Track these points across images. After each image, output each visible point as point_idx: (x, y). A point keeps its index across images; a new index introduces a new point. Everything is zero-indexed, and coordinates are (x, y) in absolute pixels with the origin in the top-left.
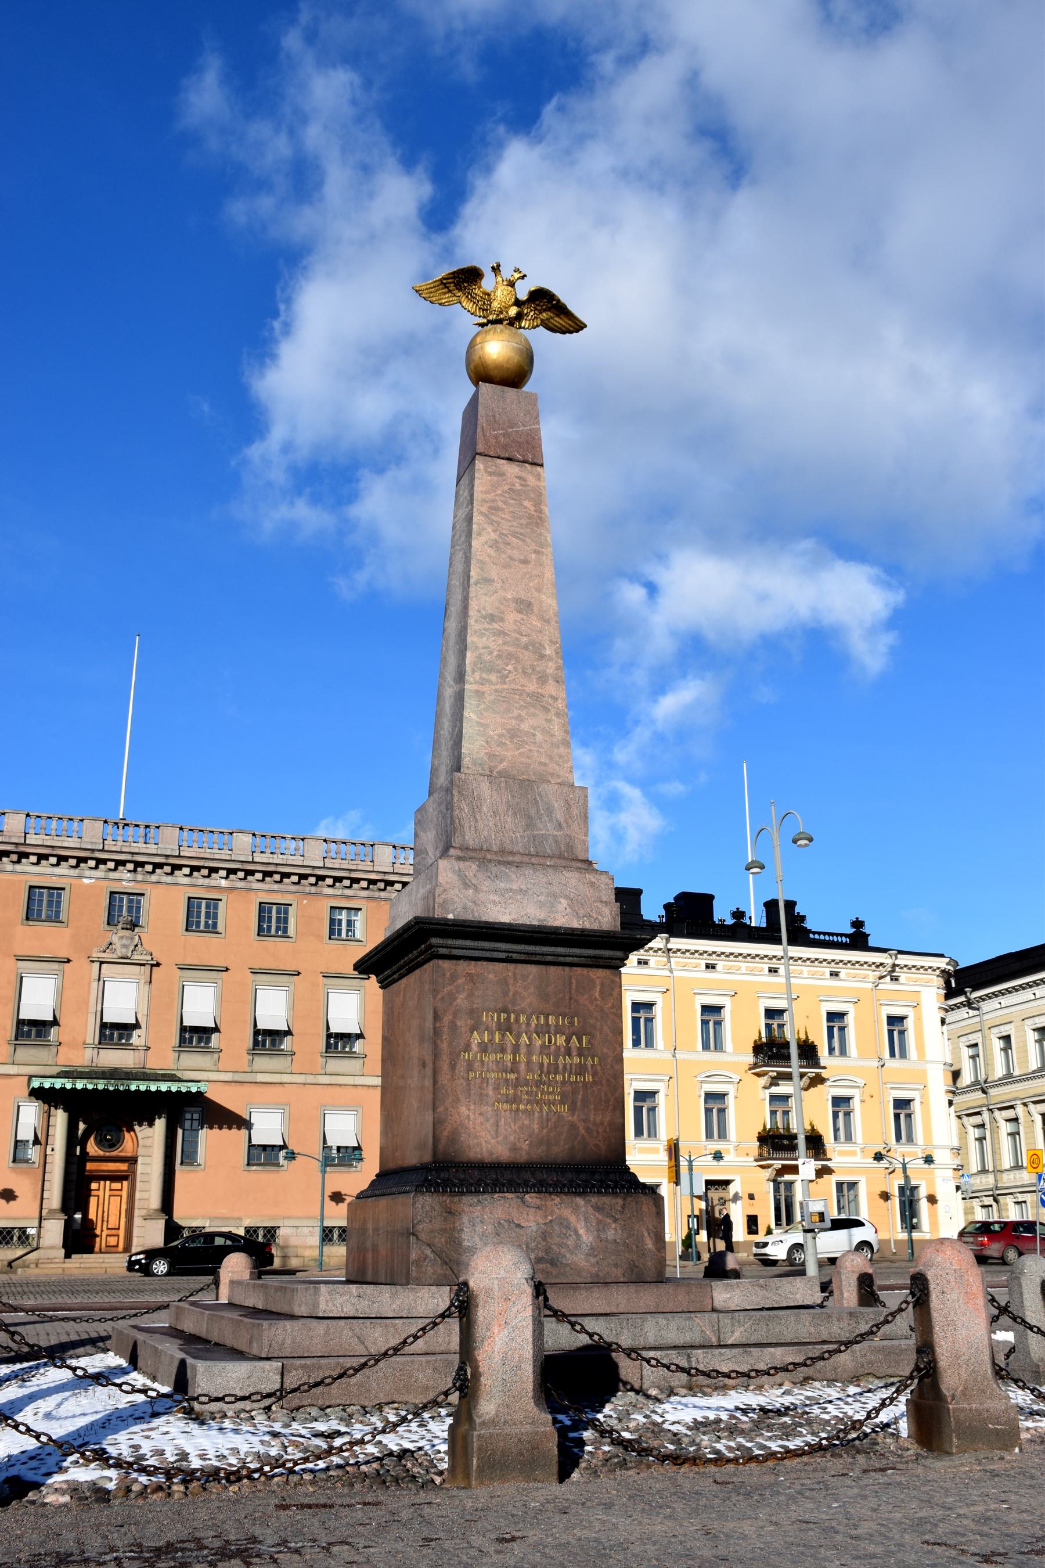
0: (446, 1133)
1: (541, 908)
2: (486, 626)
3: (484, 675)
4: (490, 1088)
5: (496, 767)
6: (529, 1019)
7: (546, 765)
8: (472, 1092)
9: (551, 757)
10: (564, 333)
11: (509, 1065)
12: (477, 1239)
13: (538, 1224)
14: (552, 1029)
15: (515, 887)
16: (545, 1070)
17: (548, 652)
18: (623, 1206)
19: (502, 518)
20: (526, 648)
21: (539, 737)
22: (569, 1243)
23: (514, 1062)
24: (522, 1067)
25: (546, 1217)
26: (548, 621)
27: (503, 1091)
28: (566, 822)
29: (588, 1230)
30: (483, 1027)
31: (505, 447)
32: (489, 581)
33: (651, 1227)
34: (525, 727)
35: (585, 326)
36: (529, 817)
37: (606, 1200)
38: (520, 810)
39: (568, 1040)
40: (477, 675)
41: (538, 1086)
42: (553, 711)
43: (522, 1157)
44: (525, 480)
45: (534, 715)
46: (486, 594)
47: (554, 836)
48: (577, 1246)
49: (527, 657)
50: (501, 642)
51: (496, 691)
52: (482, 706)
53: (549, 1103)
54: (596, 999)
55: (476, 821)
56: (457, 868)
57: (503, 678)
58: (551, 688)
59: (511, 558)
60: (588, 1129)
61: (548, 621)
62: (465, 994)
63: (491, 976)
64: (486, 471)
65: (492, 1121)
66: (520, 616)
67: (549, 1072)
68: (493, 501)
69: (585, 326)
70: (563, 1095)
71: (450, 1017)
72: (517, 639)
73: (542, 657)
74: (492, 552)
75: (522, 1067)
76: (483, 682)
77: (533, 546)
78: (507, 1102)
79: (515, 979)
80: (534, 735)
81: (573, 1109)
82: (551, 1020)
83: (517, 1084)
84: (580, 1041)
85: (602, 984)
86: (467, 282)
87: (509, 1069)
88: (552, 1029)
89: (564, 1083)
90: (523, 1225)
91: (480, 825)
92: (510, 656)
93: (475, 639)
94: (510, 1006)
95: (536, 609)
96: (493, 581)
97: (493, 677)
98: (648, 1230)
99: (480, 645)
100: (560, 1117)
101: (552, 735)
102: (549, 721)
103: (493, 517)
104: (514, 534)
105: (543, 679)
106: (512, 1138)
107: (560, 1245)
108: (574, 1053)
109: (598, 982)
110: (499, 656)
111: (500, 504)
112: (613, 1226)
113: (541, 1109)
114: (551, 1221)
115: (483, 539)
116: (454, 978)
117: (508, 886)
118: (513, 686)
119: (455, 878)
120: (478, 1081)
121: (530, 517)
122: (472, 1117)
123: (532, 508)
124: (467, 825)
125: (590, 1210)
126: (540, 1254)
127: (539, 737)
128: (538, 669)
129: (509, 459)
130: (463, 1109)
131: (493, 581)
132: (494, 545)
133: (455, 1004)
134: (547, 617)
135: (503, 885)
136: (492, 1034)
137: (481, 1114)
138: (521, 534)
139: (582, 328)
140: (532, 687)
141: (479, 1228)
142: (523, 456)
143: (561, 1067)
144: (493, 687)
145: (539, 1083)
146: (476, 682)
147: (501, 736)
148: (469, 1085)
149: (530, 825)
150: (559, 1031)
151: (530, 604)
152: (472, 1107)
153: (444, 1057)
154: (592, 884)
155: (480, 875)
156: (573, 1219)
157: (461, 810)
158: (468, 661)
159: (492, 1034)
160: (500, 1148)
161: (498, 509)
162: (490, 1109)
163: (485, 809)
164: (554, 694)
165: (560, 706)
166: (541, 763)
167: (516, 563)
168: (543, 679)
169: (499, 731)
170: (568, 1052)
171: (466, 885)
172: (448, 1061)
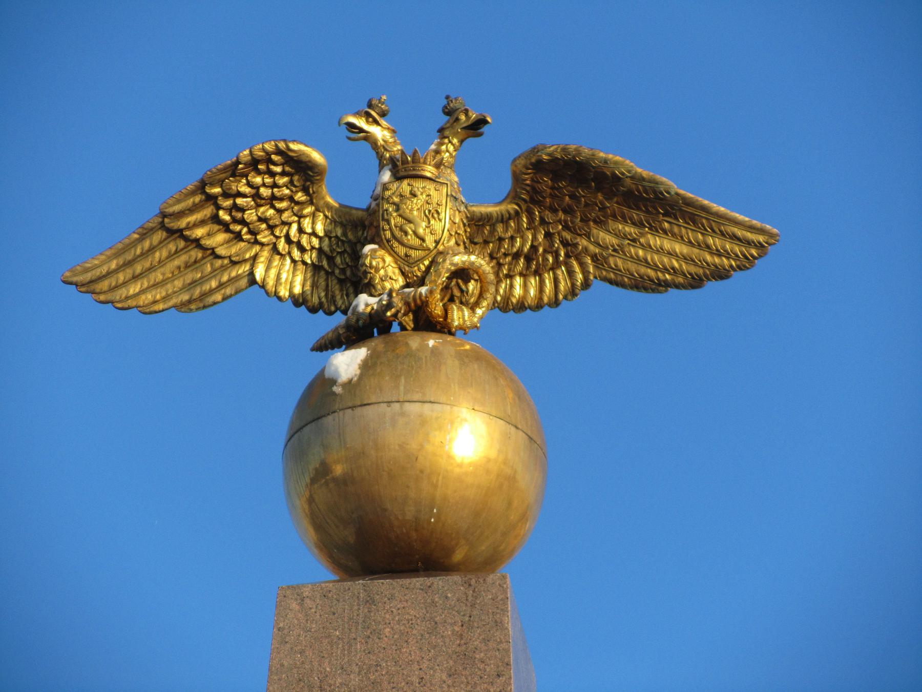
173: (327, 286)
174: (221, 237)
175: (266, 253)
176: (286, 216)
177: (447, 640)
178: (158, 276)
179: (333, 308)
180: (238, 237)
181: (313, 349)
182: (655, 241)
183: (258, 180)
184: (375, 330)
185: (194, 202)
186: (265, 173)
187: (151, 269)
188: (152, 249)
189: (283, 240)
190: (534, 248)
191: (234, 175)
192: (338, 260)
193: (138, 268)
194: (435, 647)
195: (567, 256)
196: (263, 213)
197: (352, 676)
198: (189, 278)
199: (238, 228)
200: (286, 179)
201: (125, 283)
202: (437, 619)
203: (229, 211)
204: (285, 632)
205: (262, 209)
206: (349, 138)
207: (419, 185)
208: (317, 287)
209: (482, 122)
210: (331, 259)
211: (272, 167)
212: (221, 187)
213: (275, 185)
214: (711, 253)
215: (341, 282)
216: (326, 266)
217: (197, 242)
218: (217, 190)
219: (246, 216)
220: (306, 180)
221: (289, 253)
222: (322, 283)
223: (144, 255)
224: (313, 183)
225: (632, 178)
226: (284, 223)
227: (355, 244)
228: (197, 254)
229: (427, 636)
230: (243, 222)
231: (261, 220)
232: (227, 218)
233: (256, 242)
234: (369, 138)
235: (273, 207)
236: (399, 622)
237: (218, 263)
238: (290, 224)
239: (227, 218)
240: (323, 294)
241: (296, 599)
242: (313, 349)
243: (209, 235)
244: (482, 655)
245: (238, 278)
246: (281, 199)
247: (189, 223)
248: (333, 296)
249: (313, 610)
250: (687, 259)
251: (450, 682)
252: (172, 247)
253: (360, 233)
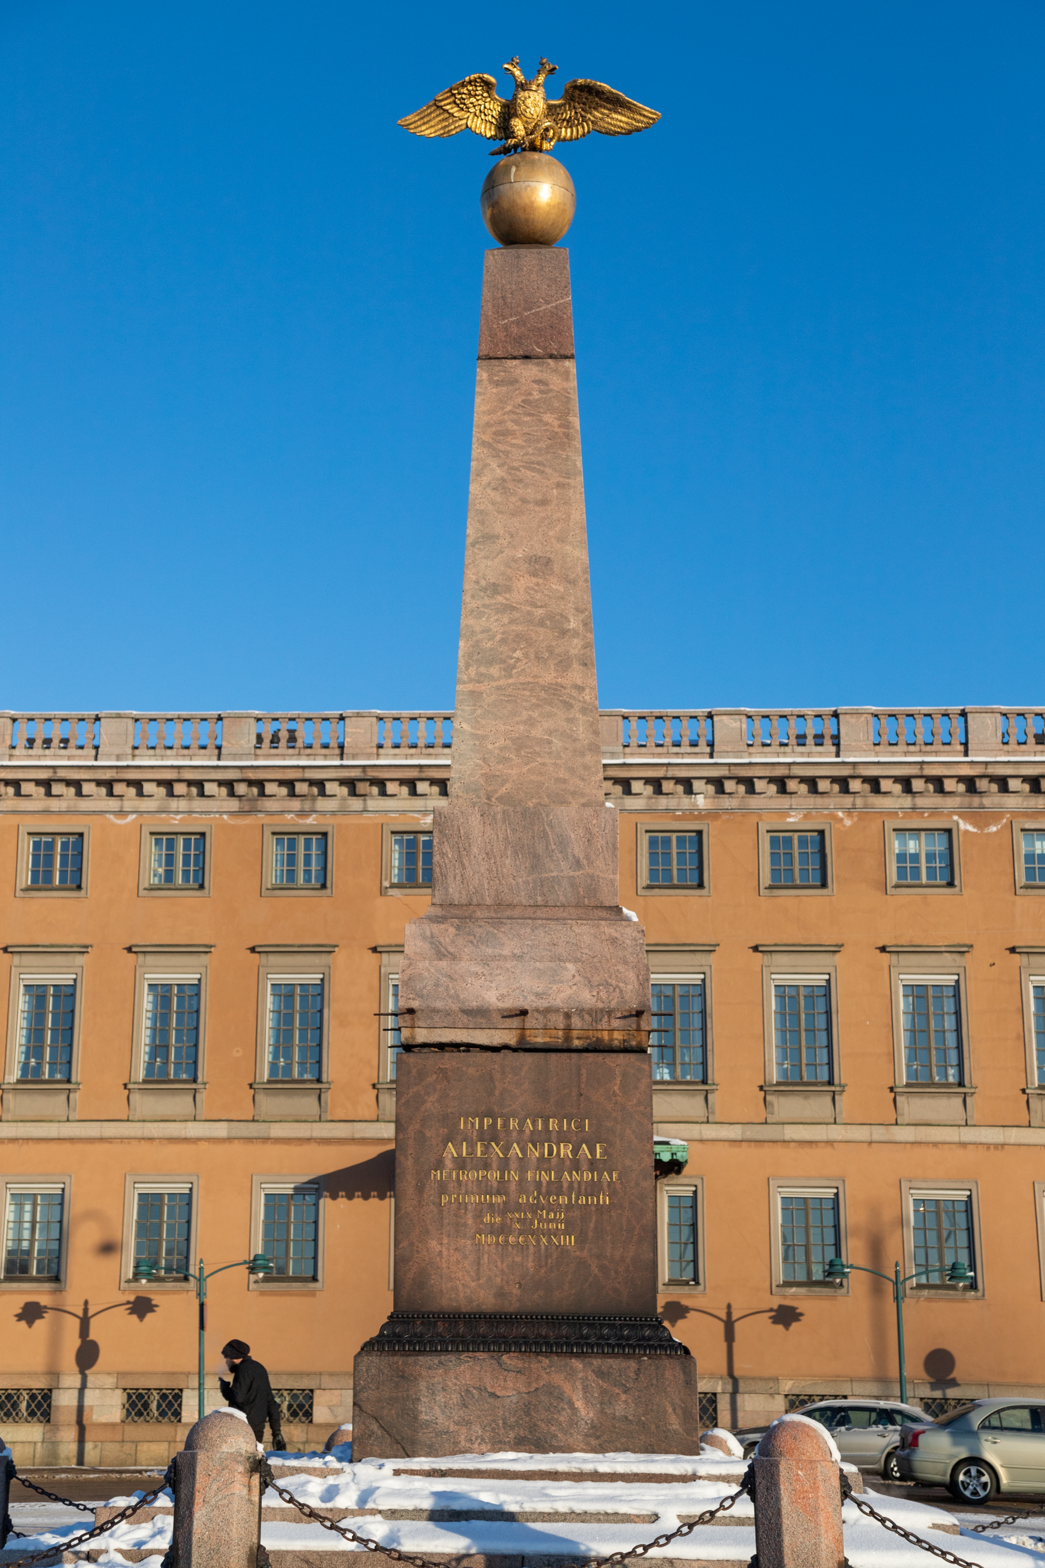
0: (410, 1275)
1: (539, 977)
2: (487, 601)
3: (483, 670)
4: (470, 1215)
5: (496, 791)
6: (522, 1124)
7: (564, 781)
8: (446, 1221)
9: (572, 770)
11: (495, 1185)
12: (437, 1411)
13: (519, 1393)
14: (554, 1136)
15: (506, 952)
16: (544, 1190)
17: (572, 625)
18: (638, 1372)
19: (513, 445)
20: (541, 623)
21: (557, 743)
22: (562, 1419)
23: (502, 1181)
24: (513, 1187)
25: (530, 1384)
26: (573, 582)
27: (487, 1219)
28: (587, 857)
29: (587, 1402)
30: (459, 1138)
31: (518, 340)
32: (490, 538)
33: (677, 1401)
34: (537, 732)
36: (536, 856)
37: (614, 1364)
38: (523, 847)
39: (575, 1151)
40: (472, 671)
41: (534, 1212)
42: (578, 706)
43: (512, 1305)
44: (546, 384)
45: (550, 715)
46: (486, 558)
47: (571, 878)
48: (573, 1423)
49: (543, 636)
50: (506, 620)
51: (498, 688)
52: (479, 712)
53: (548, 1233)
54: (615, 1094)
55: (464, 868)
56: (428, 934)
57: (508, 671)
58: (576, 675)
59: (524, 501)
60: (603, 1268)
61: (573, 582)
62: (436, 1096)
63: (471, 1071)
64: (491, 381)
65: (472, 1258)
66: (534, 580)
67: (549, 1193)
68: (501, 423)
70: (568, 1222)
71: (417, 1126)
72: (529, 613)
73: (564, 633)
74: (497, 497)
75: (513, 1187)
76: (480, 678)
77: (556, 478)
78: (491, 1233)
79: (503, 1073)
80: (549, 742)
81: (581, 1241)
82: (553, 1124)
83: (505, 1209)
84: (592, 1151)
85: (624, 1075)
87: (494, 1191)
88: (554, 1136)
89: (569, 1207)
90: (498, 1394)
91: (469, 872)
92: (519, 637)
93: (471, 621)
94: (496, 1108)
95: (556, 568)
96: (498, 537)
97: (495, 671)
98: (673, 1404)
99: (478, 629)
100: (563, 1251)
101: (575, 740)
102: (570, 721)
103: (500, 447)
104: (529, 466)
105: (564, 664)
106: (499, 1280)
107: (549, 1422)
108: (585, 1166)
109: (617, 1071)
110: (503, 641)
111: (510, 425)
112: (623, 1397)
113: (538, 1241)
114: (537, 1389)
115: (485, 480)
116: (421, 1075)
117: (497, 951)
118: (522, 679)
119: (427, 946)
120: (454, 1206)
121: (554, 436)
122: (445, 1253)
123: (556, 423)
124: (451, 875)
125: (591, 1376)
126: (521, 1433)
127: (557, 743)
128: (557, 651)
129: (526, 357)
130: (433, 1244)
131: (498, 537)
132: (501, 486)
133: (423, 1109)
134: (572, 576)
135: (490, 951)
136: (472, 1146)
137: (456, 1249)
138: (538, 463)
140: (549, 677)
141: (440, 1398)
142: (545, 348)
143: (565, 1185)
144: (494, 684)
145: (535, 1208)
146: (471, 680)
147: (501, 749)
148: (441, 1212)
149: (536, 864)
150: (562, 1137)
151: (549, 561)
152: (445, 1241)
153: (408, 1177)
154: (613, 941)
155: (460, 941)
156: (567, 1388)
157: (443, 855)
158: (460, 653)
159: (472, 1146)
160: (482, 1293)
161: (506, 433)
162: (469, 1242)
163: (475, 850)
164: (579, 682)
165: (587, 698)
166: (558, 780)
167: (531, 506)
168: (564, 664)
169: (501, 742)
170: (576, 1165)
171: (440, 955)
172: (414, 1182)
174: (456, 109)
175: (472, 116)
176: (480, 102)
178: (432, 123)
180: (462, 109)
183: (470, 88)
187: (430, 121)
193: (426, 120)
198: (444, 124)
207: (531, 93)
209: (554, 69)
217: (447, 111)
223: (429, 115)
228: (446, 115)
234: (513, 74)
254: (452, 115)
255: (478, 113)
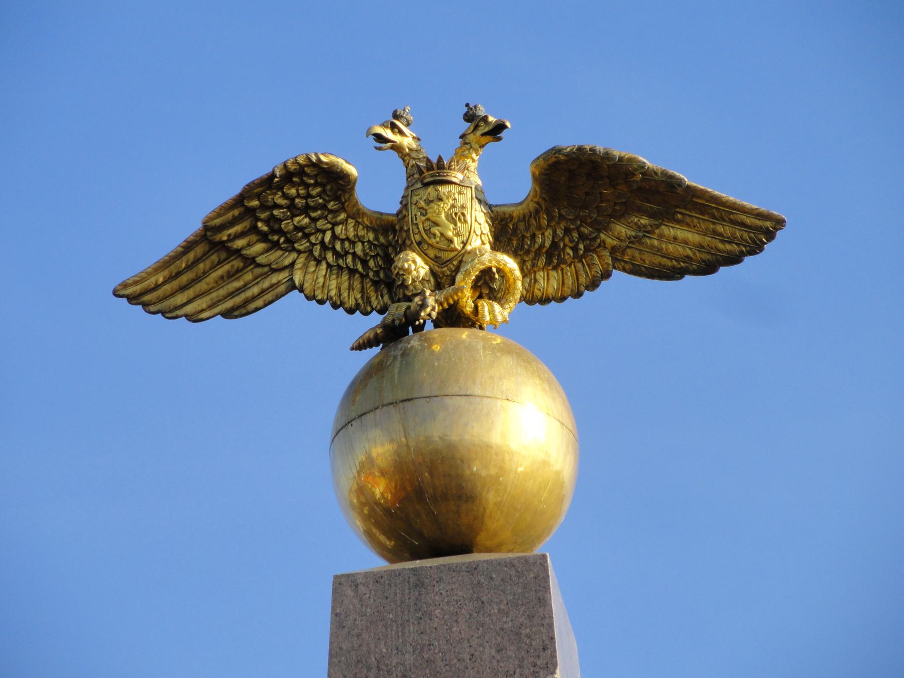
10: (708, 268)
35: (780, 223)
69: (780, 223)
86: (306, 210)
139: (770, 236)
173: (363, 287)
174: (260, 247)
175: (301, 260)
176: (320, 224)
177: (494, 618)
178: (202, 286)
179: (369, 309)
180: (275, 245)
181: (352, 349)
182: (669, 231)
183: (293, 191)
184: (410, 328)
185: (233, 216)
186: (299, 185)
188: (196, 262)
189: (318, 247)
190: (554, 244)
191: (270, 188)
192: (371, 263)
193: (184, 279)
194: (483, 625)
195: (587, 249)
196: (299, 222)
197: (407, 656)
199: (276, 238)
200: (318, 190)
201: (173, 294)
202: (484, 599)
203: (267, 222)
204: (342, 617)
205: (297, 219)
206: (376, 148)
208: (353, 290)
209: (500, 127)
210: (365, 263)
211: (305, 179)
212: (259, 200)
213: (308, 196)
214: (722, 241)
215: (376, 284)
216: (360, 269)
217: (238, 252)
218: (255, 203)
219: (283, 226)
220: (339, 189)
221: (325, 258)
222: (357, 284)
223: (189, 268)
224: (344, 191)
225: (643, 174)
226: (318, 231)
227: (387, 247)
228: (237, 263)
229: (475, 615)
230: (281, 232)
231: (298, 229)
232: (265, 228)
233: (294, 249)
235: (308, 216)
236: (448, 603)
237: (258, 271)
238: (324, 232)
239: (265, 228)
240: (359, 296)
241: (351, 586)
242: (352, 349)
243: (249, 245)
244: (528, 630)
245: (278, 283)
246: (315, 209)
247: (229, 235)
248: (368, 298)
249: (367, 596)
250: (700, 247)
251: (499, 657)
252: (214, 258)
253: (391, 237)
254: (251, 261)
255: (317, 252)
